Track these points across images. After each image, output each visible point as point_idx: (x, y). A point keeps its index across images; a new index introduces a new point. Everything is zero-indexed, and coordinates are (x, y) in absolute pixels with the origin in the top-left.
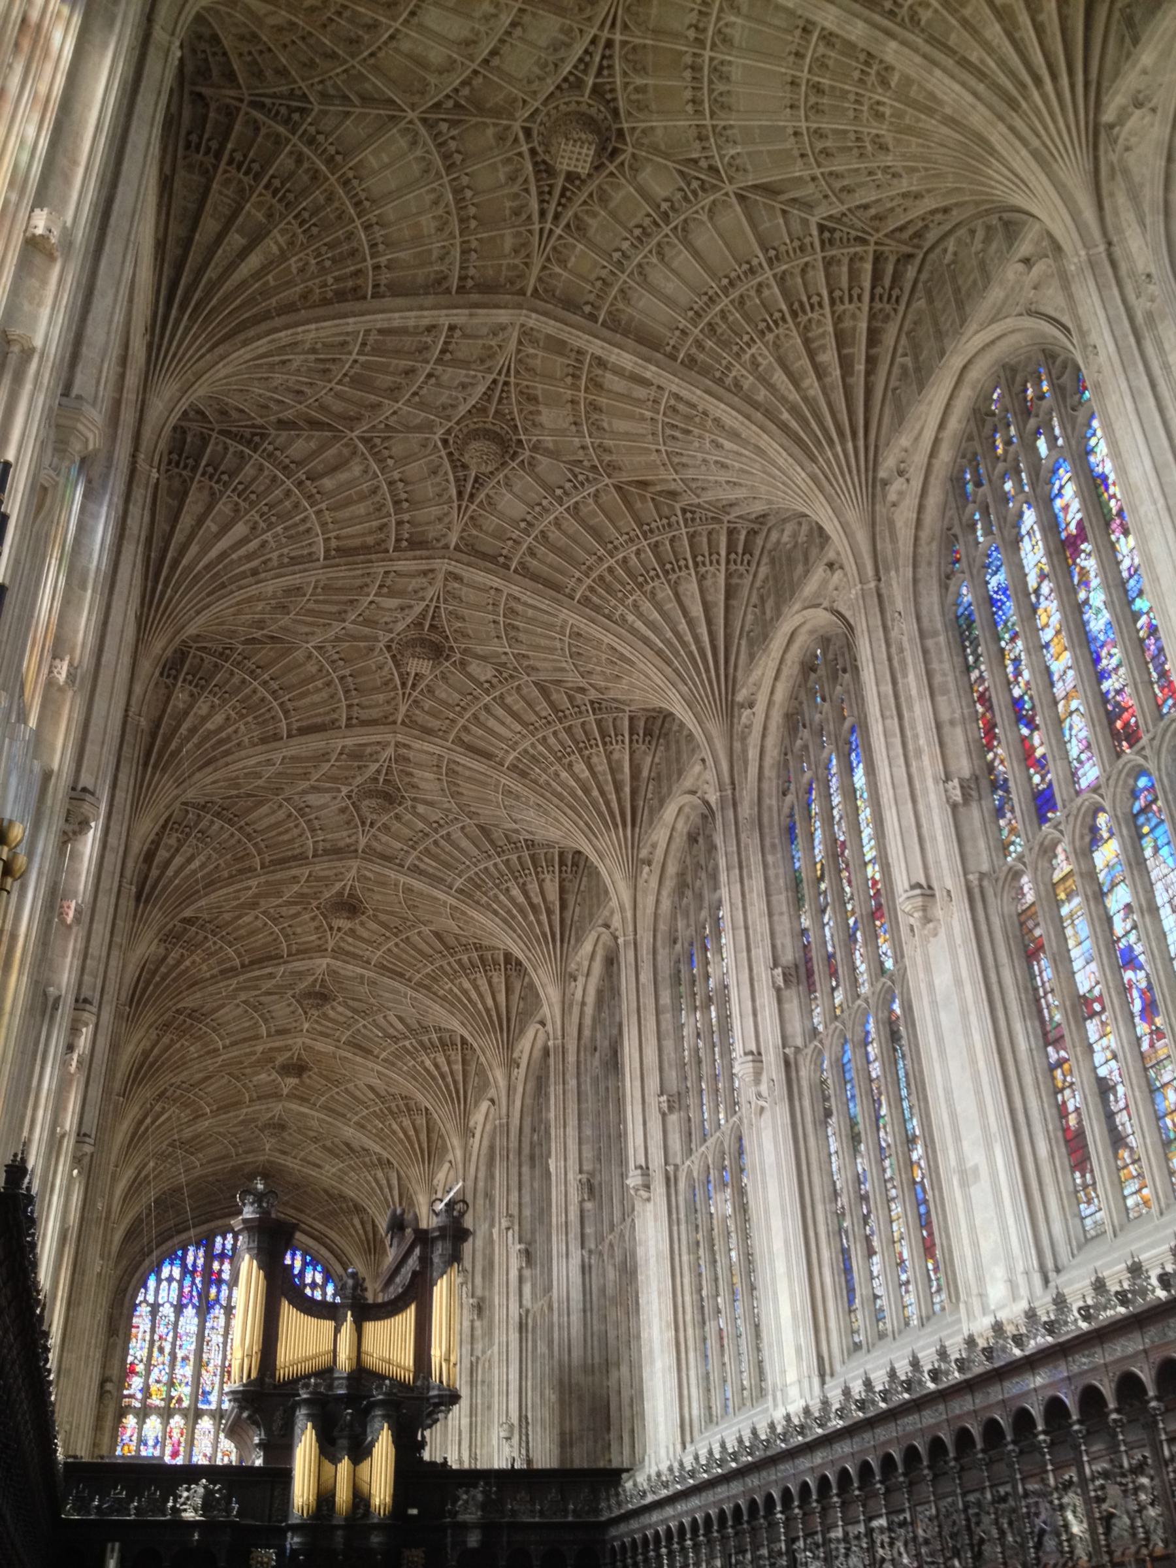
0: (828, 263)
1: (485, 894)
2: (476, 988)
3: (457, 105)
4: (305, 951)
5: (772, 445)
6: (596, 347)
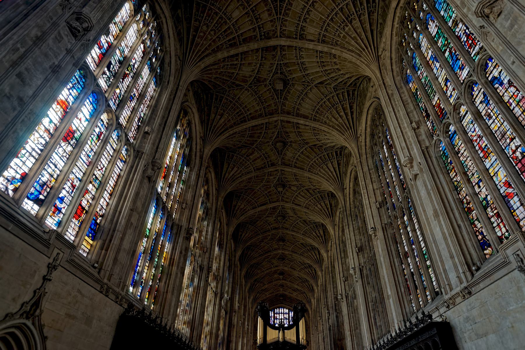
0: (337, 95)
3: (255, 83)
5: (335, 133)
6: (295, 121)
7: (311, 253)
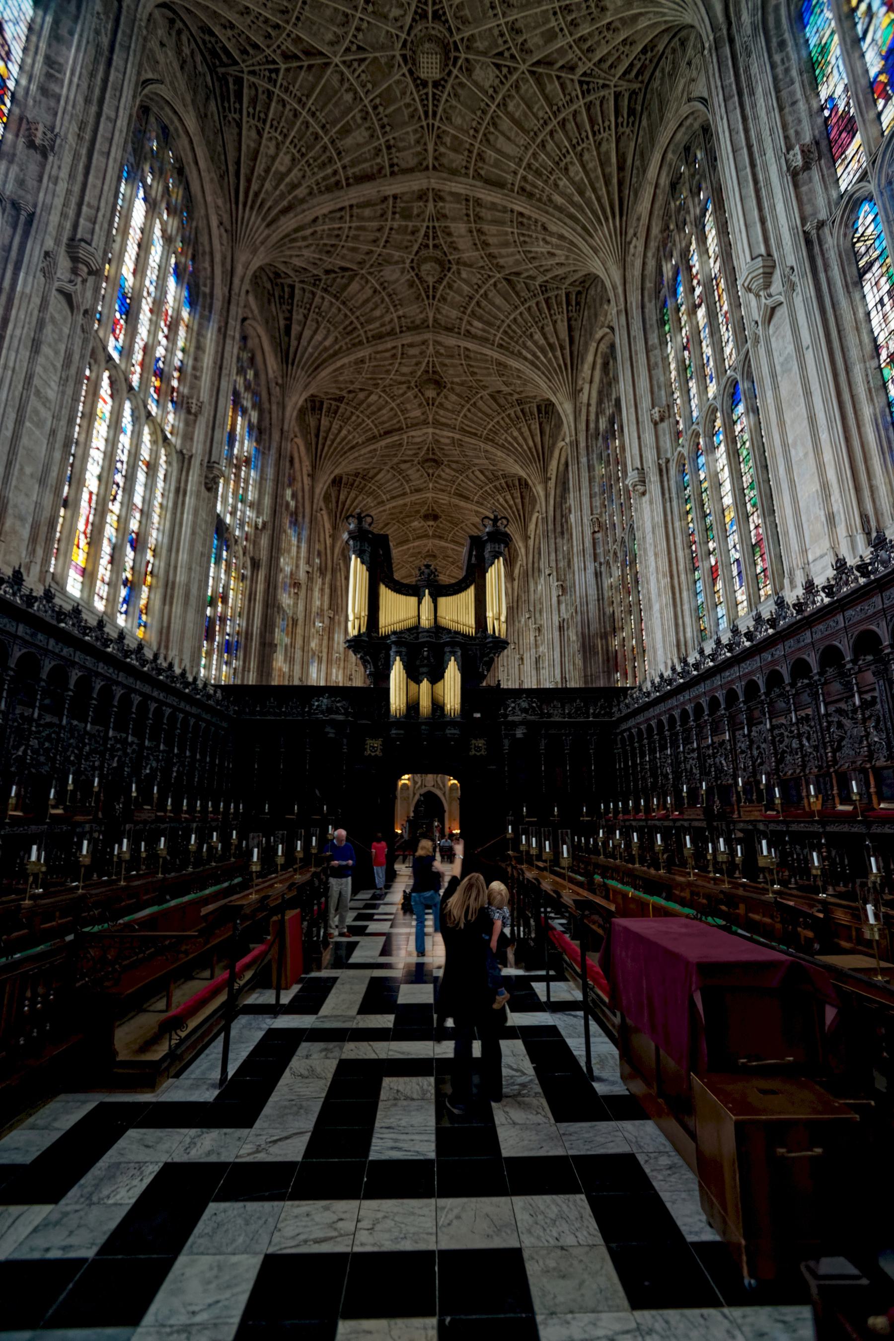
1: (517, 342)
2: (522, 434)
4: (417, 424)
7: (519, 430)
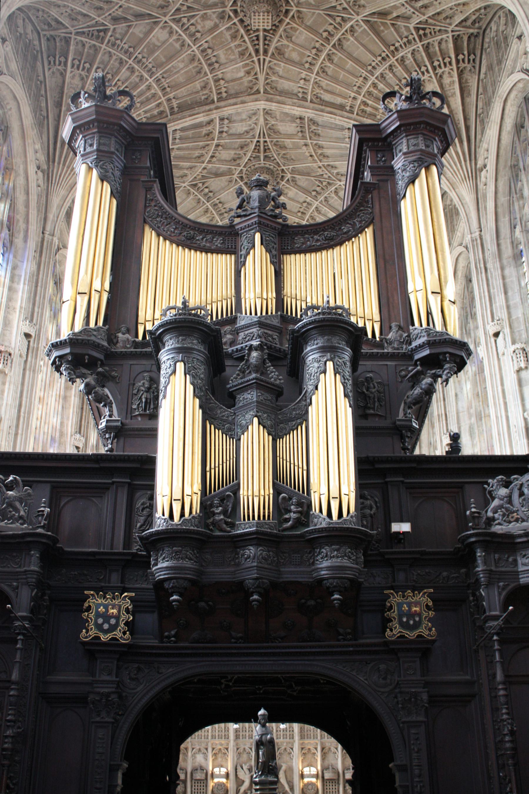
4: (236, 95)
